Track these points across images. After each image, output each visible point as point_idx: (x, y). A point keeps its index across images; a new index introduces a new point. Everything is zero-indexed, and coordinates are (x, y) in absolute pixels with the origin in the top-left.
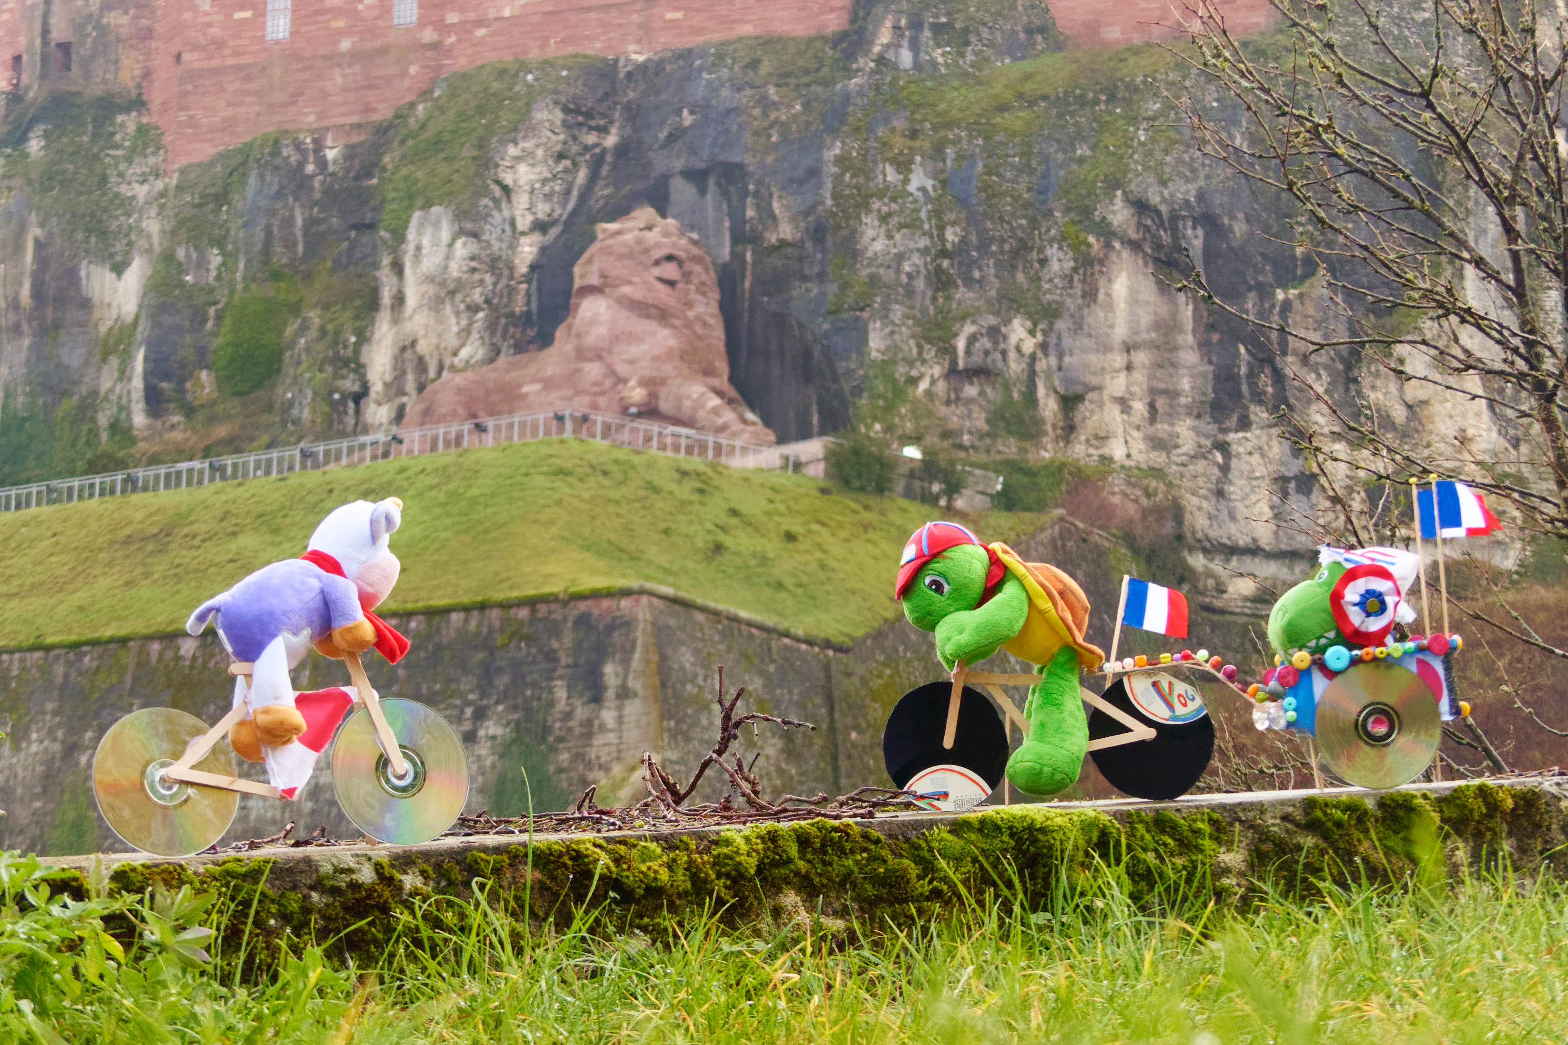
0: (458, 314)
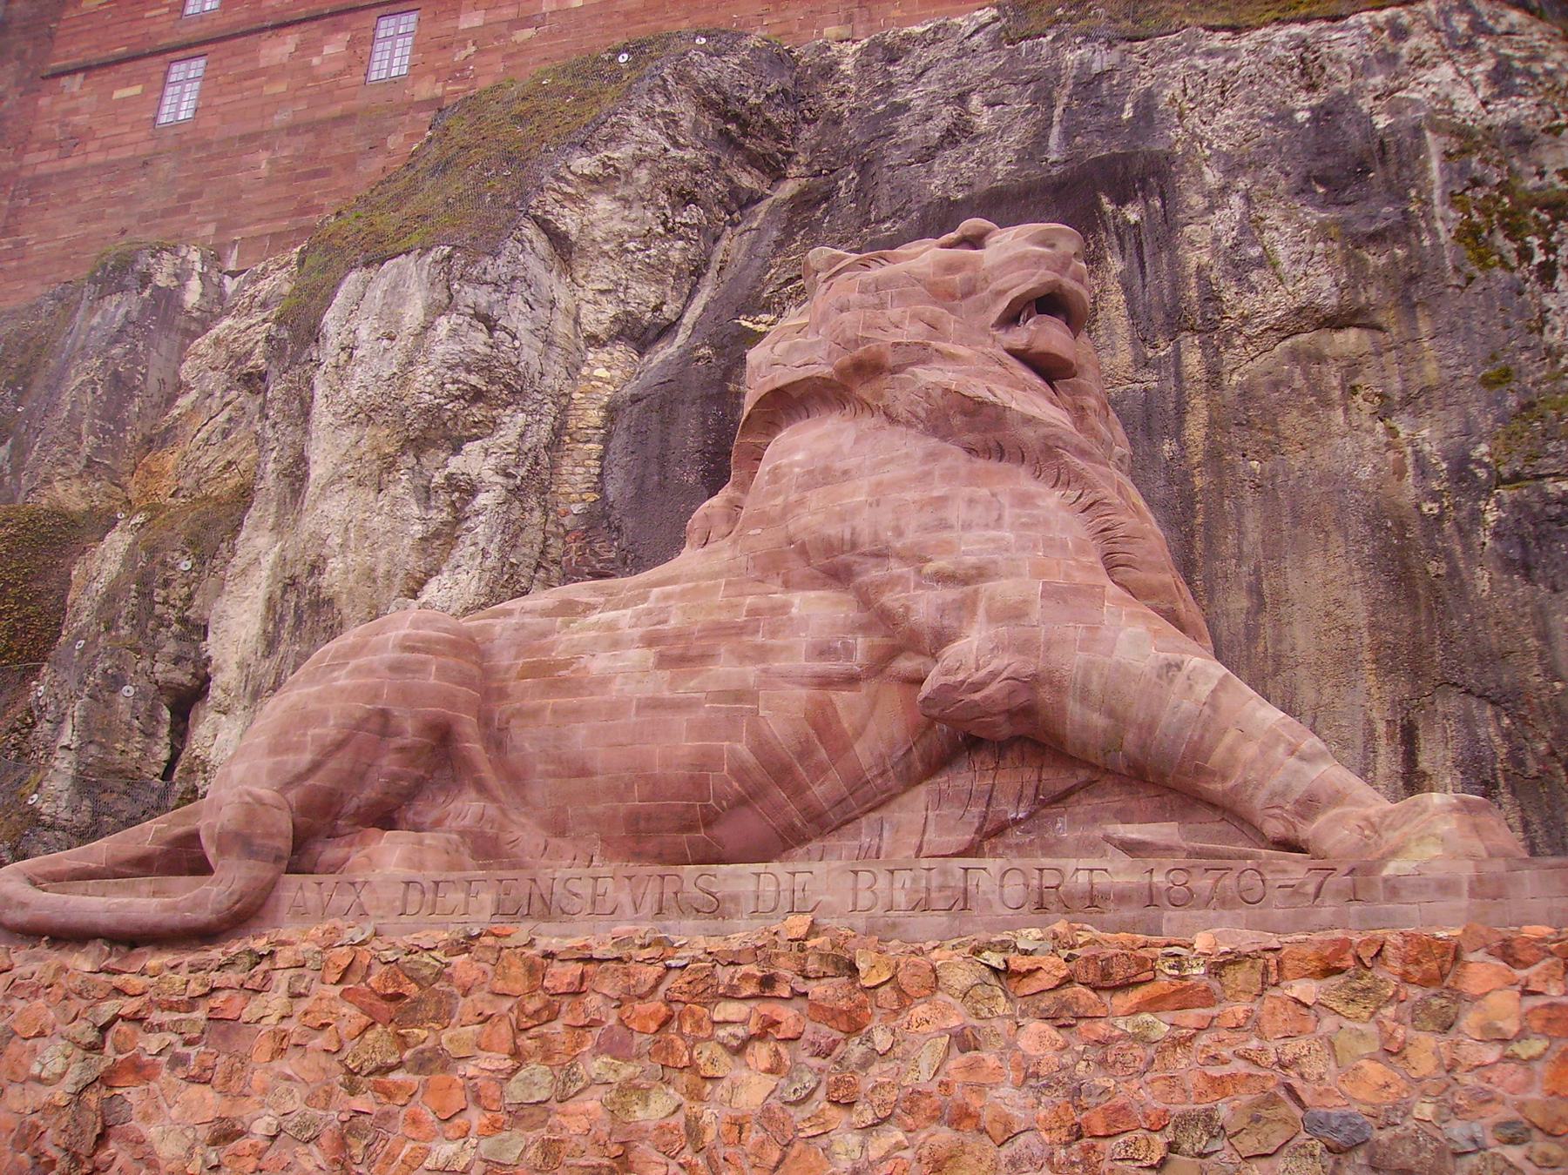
0: (426, 495)
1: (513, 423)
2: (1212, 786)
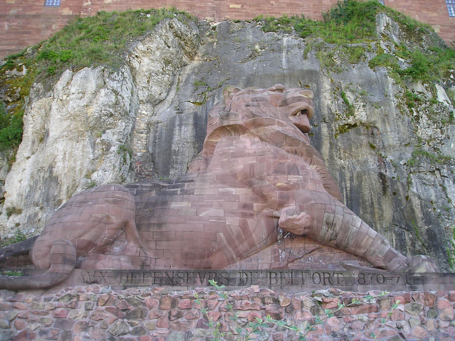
0: (94, 145)
1: (121, 125)
2: (360, 251)
